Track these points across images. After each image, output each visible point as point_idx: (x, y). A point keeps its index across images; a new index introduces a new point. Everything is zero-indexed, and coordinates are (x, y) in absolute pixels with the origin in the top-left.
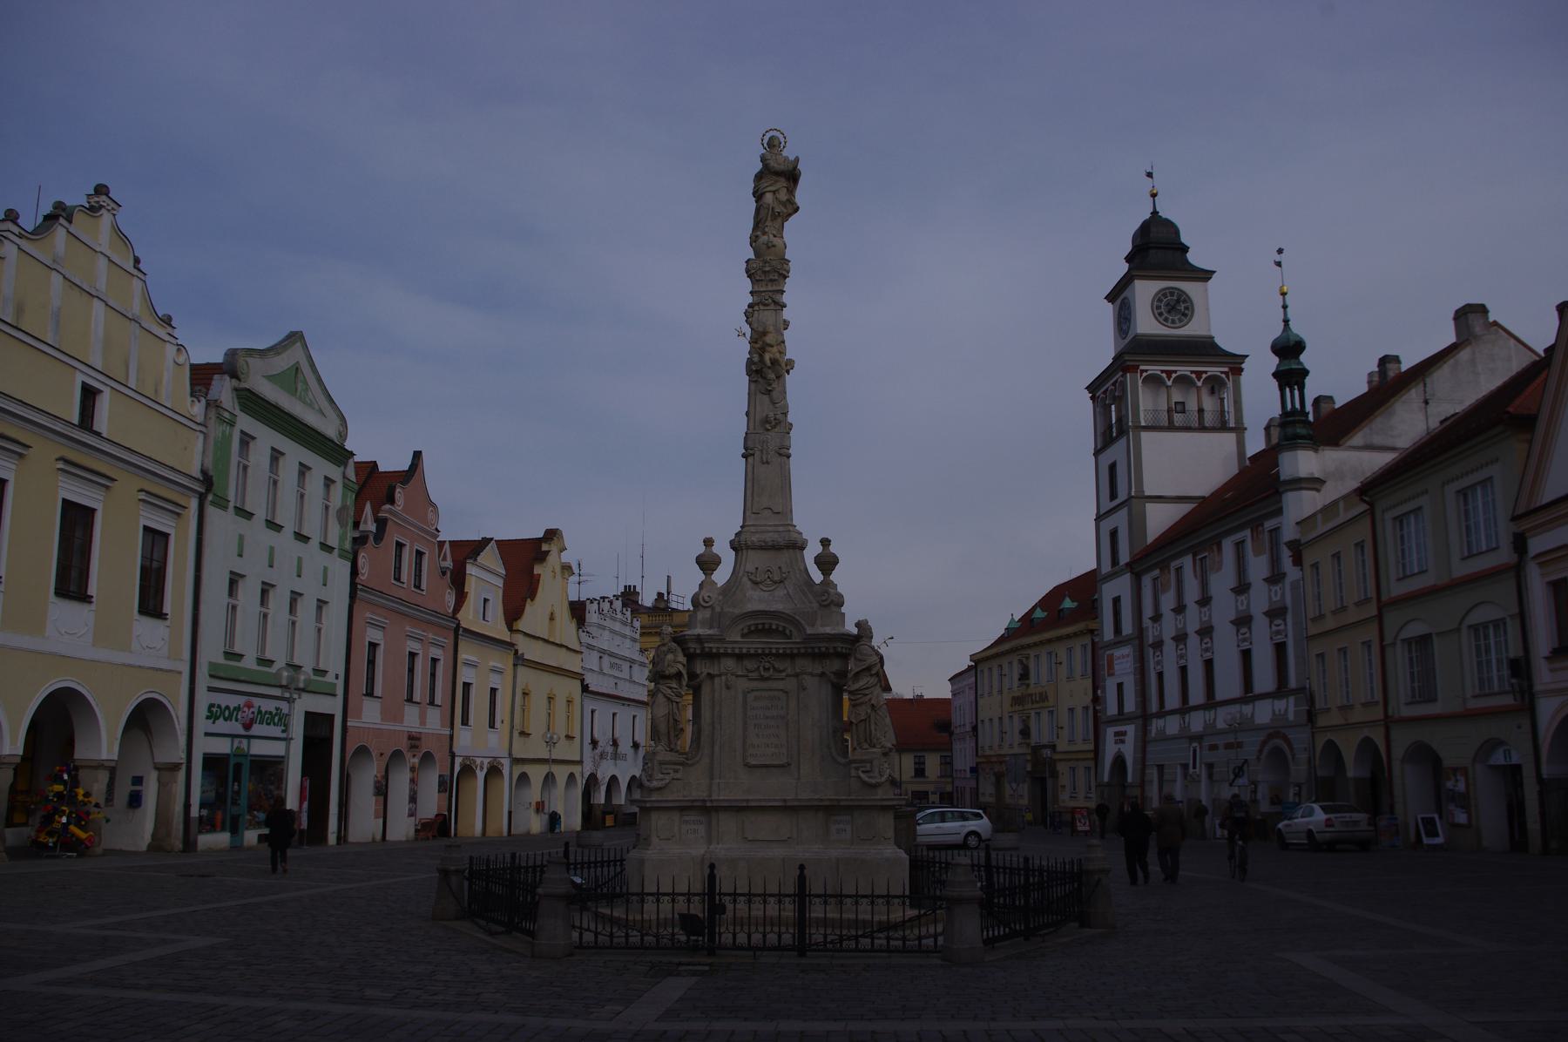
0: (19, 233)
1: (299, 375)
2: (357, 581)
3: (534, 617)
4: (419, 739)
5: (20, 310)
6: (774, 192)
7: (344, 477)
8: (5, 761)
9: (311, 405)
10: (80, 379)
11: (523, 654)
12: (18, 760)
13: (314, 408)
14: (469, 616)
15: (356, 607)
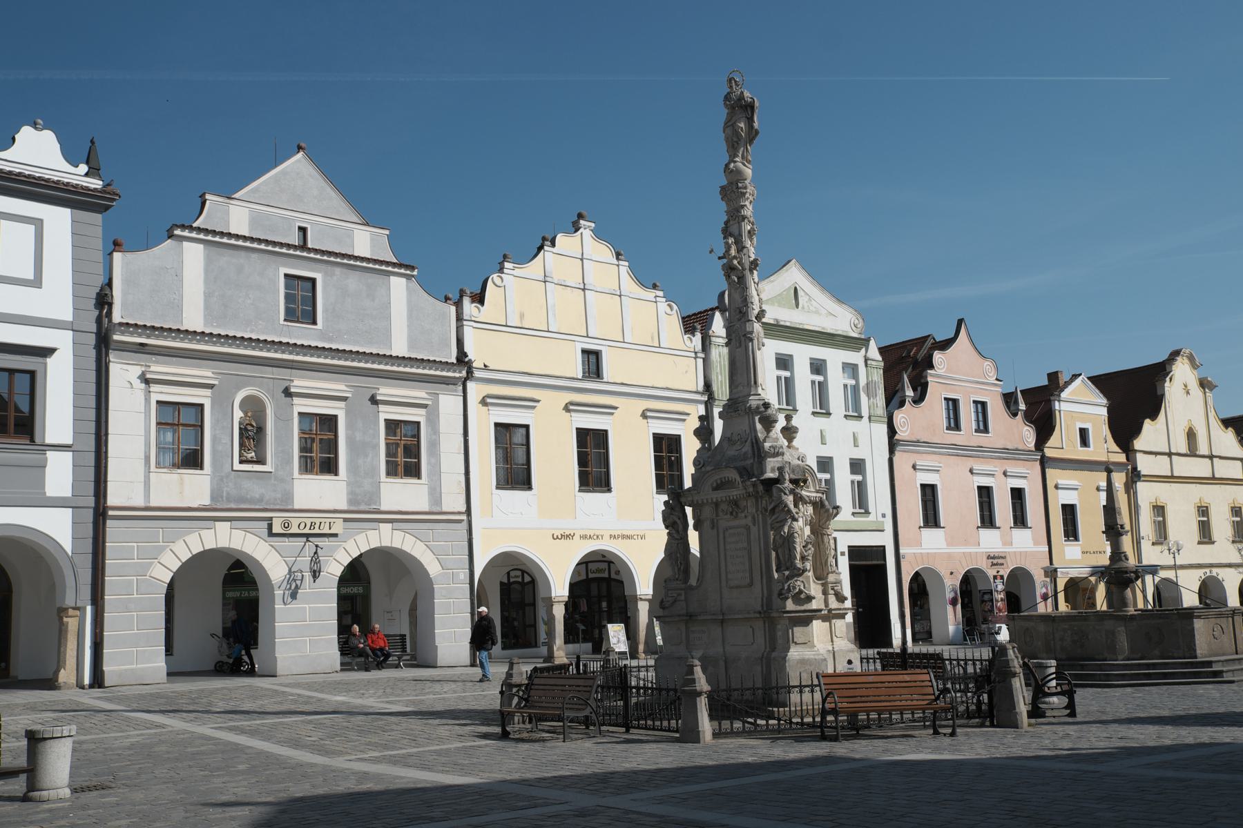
0: (514, 267)
1: (800, 293)
2: (897, 437)
3: (1150, 435)
4: (1003, 558)
5: (522, 316)
6: (732, 125)
7: (866, 360)
8: (556, 600)
9: (817, 312)
10: (579, 347)
11: (1139, 471)
12: (567, 599)
13: (820, 314)
14: (1063, 443)
15: (895, 459)
